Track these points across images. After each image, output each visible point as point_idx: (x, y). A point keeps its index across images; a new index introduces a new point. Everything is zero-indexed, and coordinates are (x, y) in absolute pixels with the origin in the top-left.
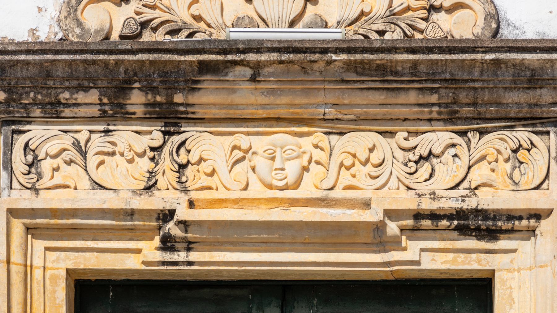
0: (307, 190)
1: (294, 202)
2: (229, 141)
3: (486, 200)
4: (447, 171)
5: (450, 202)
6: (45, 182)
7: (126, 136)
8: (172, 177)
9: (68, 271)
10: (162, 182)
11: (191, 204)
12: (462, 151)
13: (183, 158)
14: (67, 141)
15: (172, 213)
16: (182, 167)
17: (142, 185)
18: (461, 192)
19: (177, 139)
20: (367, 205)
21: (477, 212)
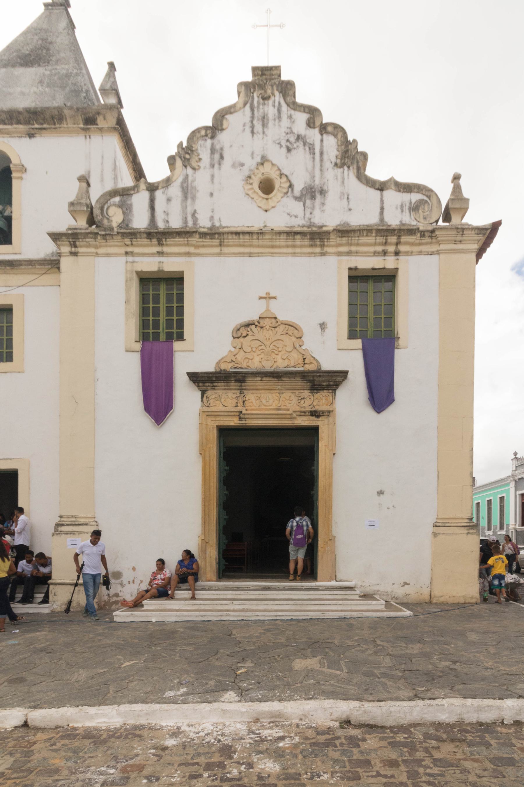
0: (274, 406)
1: (271, 409)
2: (255, 395)
3: (317, 408)
4: (308, 402)
5: (309, 409)
6: (211, 405)
7: (230, 394)
8: (242, 404)
9: (217, 426)
10: (239, 405)
11: (246, 410)
12: (312, 397)
13: (244, 399)
14: (216, 395)
15: (241, 412)
16: (244, 401)
17: (235, 405)
18: (311, 407)
19: (243, 395)
20: (288, 410)
21: (315, 411)
